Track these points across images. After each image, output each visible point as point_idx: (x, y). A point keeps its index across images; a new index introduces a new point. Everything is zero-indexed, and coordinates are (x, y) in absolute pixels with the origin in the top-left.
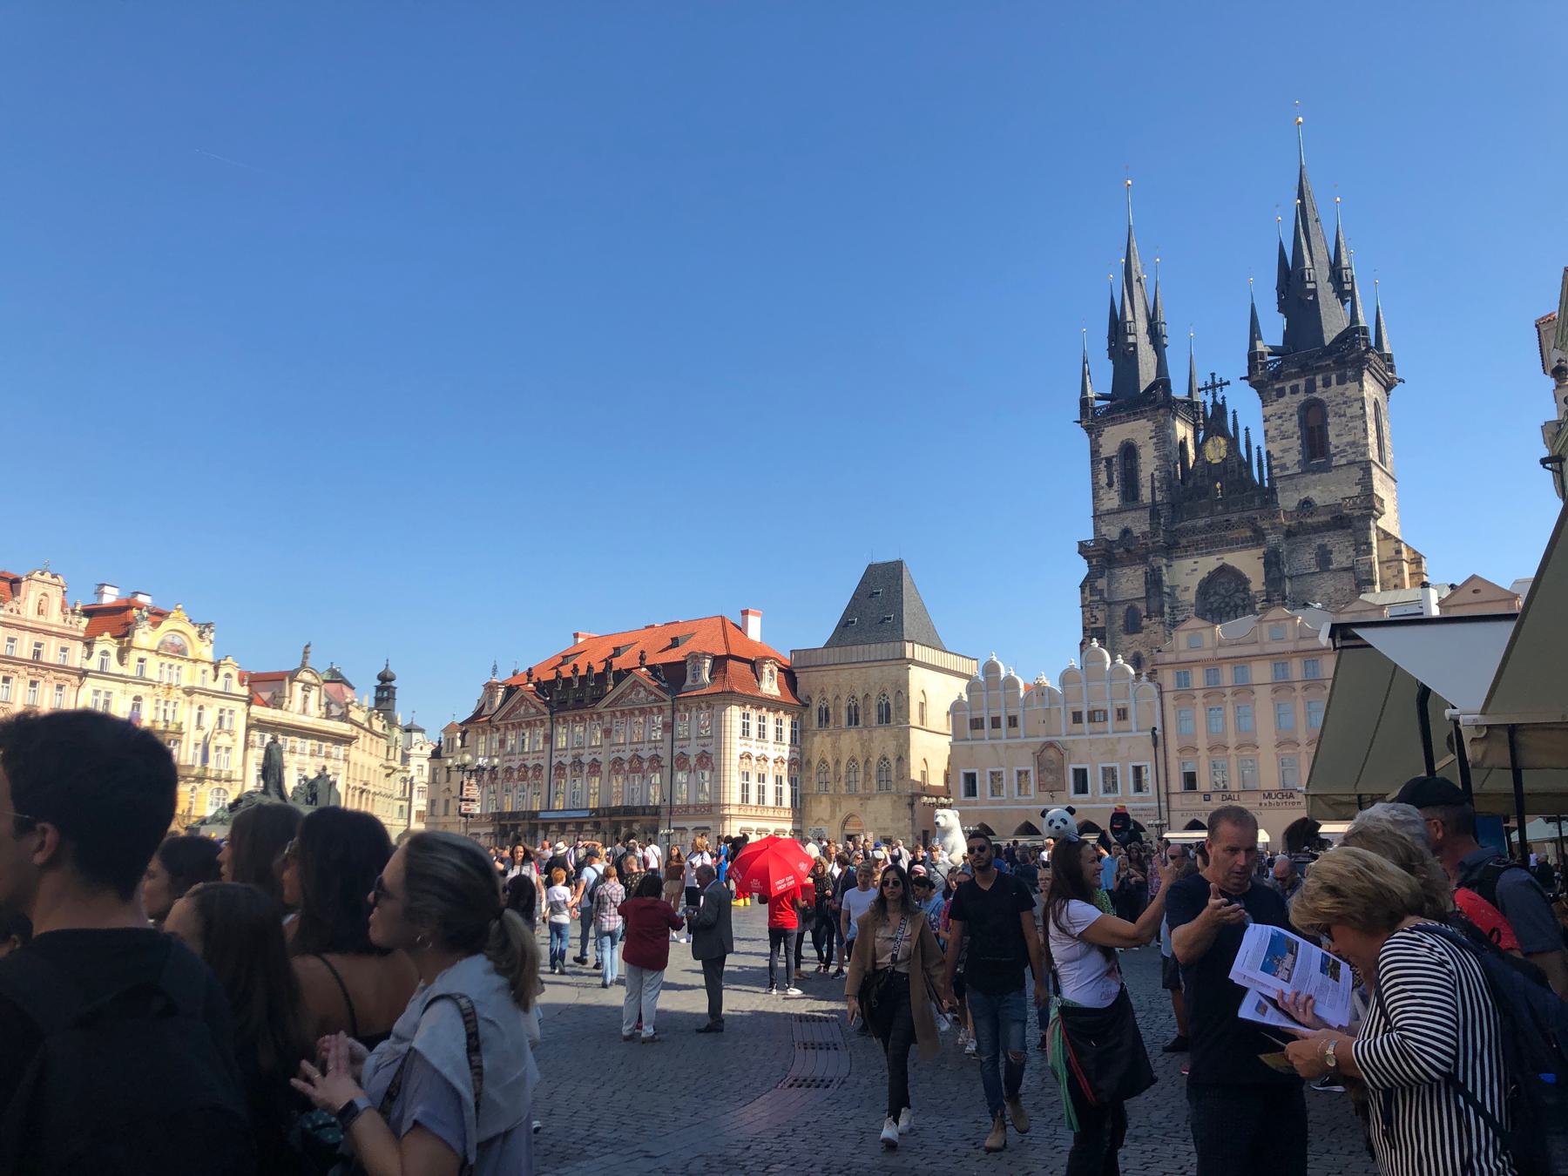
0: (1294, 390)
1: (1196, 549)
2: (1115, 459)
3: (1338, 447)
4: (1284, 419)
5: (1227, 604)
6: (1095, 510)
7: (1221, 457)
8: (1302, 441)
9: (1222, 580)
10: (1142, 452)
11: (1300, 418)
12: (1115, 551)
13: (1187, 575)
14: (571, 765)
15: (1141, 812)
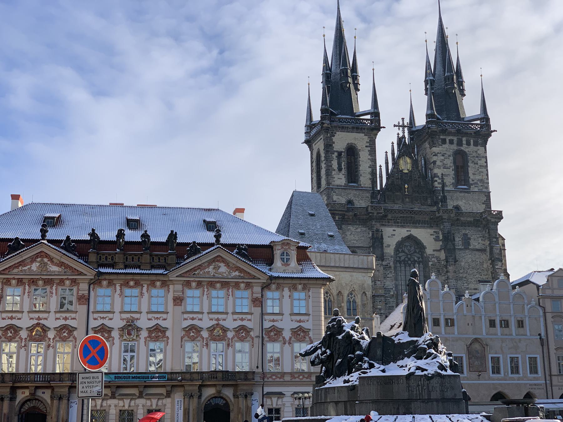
0: (451, 142)
1: (395, 223)
2: (343, 154)
3: (473, 181)
4: (445, 157)
5: (409, 259)
6: (328, 183)
7: (408, 170)
8: (455, 172)
9: (407, 244)
10: (361, 153)
11: (454, 158)
12: (346, 214)
13: (389, 237)
14: (122, 329)
15: (534, 387)
